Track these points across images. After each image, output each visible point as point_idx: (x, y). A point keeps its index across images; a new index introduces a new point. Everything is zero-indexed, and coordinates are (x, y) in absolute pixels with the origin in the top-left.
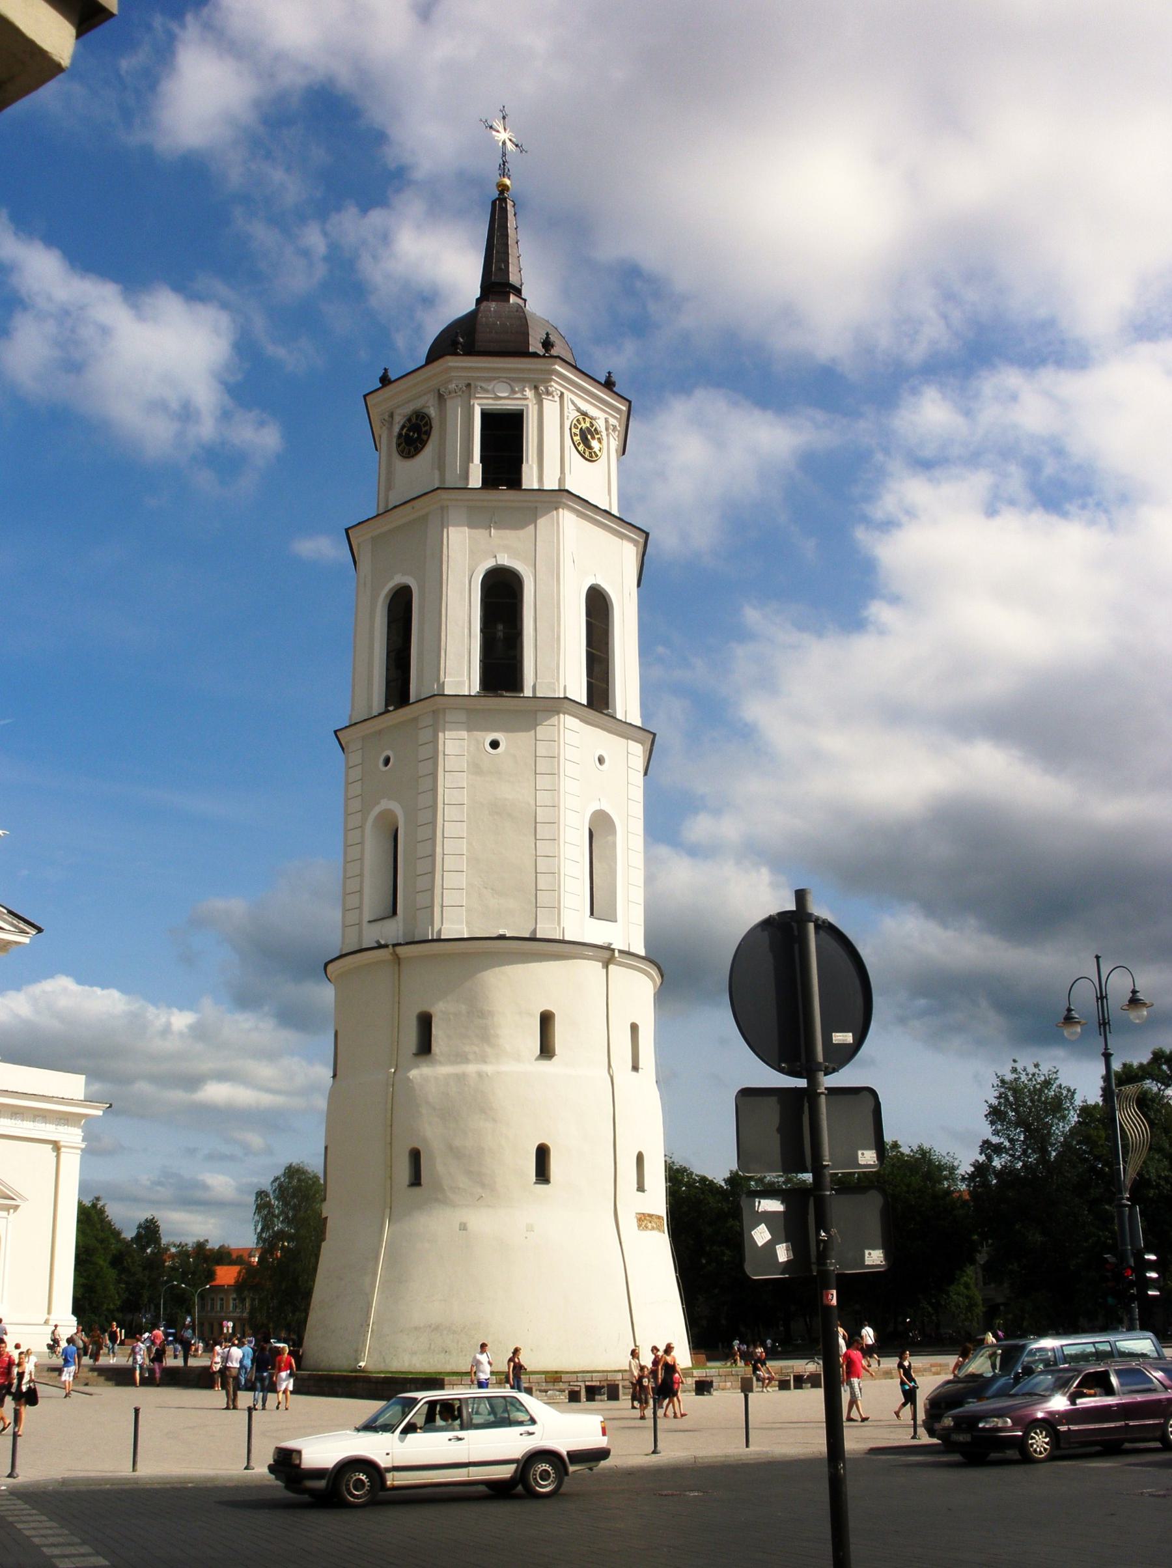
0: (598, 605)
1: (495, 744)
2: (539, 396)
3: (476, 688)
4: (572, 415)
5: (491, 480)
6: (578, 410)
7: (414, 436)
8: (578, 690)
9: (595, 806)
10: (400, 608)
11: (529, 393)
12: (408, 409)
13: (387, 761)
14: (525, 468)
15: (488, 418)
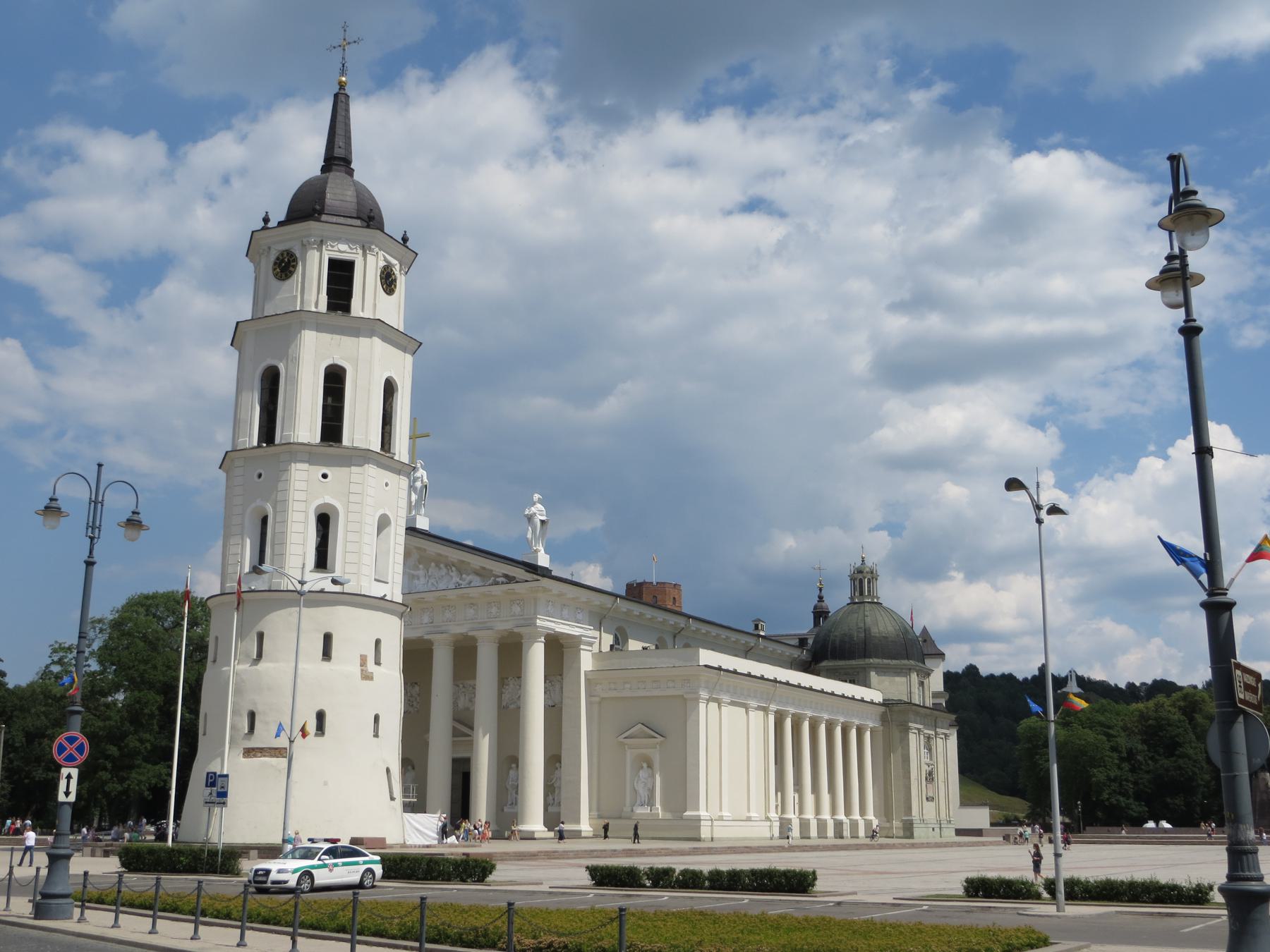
0: (390, 389)
1: (325, 476)
2: (365, 255)
3: (318, 439)
4: (382, 264)
5: (332, 307)
6: (385, 260)
7: (285, 266)
8: (376, 447)
9: (381, 512)
10: (271, 384)
11: (360, 251)
12: (283, 247)
13: (260, 476)
14: (353, 300)
15: (334, 264)
